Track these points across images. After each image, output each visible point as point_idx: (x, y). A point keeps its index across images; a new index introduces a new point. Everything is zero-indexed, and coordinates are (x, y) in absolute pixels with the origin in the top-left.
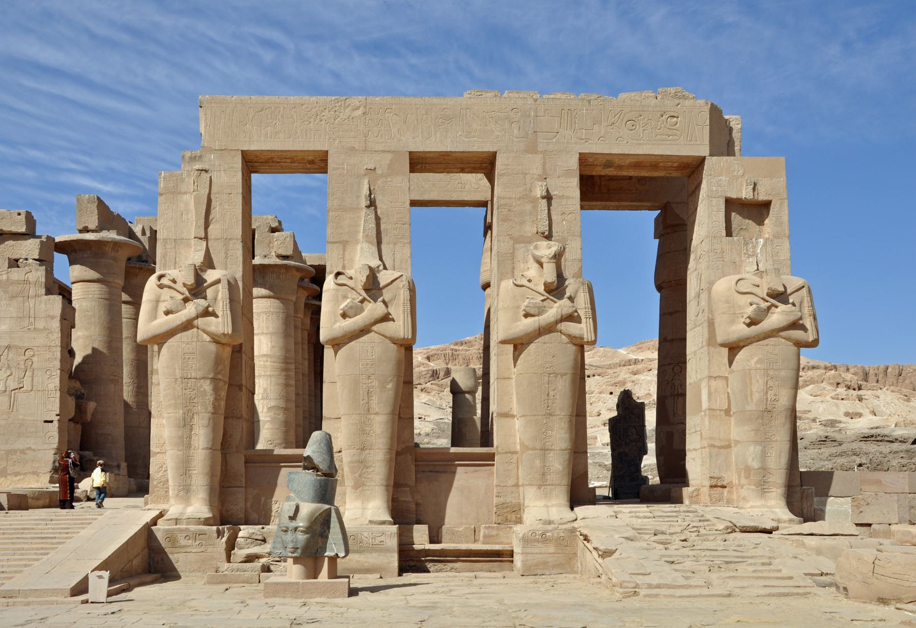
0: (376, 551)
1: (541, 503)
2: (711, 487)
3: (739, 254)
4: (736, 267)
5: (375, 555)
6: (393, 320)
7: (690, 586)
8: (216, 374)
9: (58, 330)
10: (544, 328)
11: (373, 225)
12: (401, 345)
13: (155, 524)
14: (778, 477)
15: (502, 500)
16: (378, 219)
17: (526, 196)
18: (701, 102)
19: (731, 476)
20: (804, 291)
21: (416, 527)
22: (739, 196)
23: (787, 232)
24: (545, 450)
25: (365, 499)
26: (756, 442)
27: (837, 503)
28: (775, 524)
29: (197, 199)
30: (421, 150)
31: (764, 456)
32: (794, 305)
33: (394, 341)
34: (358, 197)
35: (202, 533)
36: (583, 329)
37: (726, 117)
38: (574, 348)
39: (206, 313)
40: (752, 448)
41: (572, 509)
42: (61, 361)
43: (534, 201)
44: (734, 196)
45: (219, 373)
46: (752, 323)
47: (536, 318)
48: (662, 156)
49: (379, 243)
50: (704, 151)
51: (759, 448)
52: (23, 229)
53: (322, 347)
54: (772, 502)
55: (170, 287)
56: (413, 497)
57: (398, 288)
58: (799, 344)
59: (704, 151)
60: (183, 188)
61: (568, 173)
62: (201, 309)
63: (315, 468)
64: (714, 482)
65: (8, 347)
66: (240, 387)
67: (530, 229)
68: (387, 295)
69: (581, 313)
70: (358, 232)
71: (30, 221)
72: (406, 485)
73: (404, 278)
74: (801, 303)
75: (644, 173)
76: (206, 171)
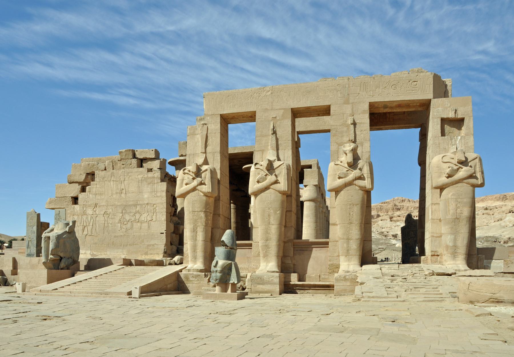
0: (270, 284)
1: (346, 263)
2: (432, 256)
3: (448, 145)
4: (446, 150)
5: (269, 285)
6: (279, 183)
7: (389, 297)
8: (206, 209)
9: (165, 196)
10: (347, 183)
11: (275, 142)
12: (284, 194)
13: (181, 272)
14: (462, 250)
15: (332, 262)
16: (277, 140)
17: (344, 124)
18: (429, 73)
19: (440, 251)
20: (477, 160)
21: (292, 274)
22: (448, 117)
23: (472, 132)
24: (348, 239)
25: (268, 261)
26: (451, 234)
27: (496, 263)
28: (454, 272)
29: (202, 137)
30: (296, 107)
31: (455, 240)
32: (471, 167)
33: (280, 192)
34: (269, 130)
35: (199, 276)
36: (366, 183)
37: (443, 80)
38: (362, 192)
39: (201, 184)
40: (449, 237)
41: (361, 266)
42: (167, 209)
43: (348, 126)
44: (445, 117)
45: (208, 209)
46: (449, 176)
47: (344, 179)
48: (410, 100)
49: (278, 150)
50: (430, 96)
51: (453, 236)
52: (154, 157)
53: (302, 203)
54: (459, 262)
55: (188, 174)
56: (292, 261)
57: (282, 169)
58: (474, 186)
59: (430, 96)
60: (197, 132)
61: (364, 112)
62: (199, 182)
63: (226, 246)
64: (433, 253)
65: (148, 204)
66: (219, 215)
67: (346, 139)
68: (277, 172)
69: (365, 175)
70: (268, 146)
71: (157, 153)
72: (289, 256)
73: (285, 164)
74: (475, 166)
75: (405, 110)
76: (206, 124)
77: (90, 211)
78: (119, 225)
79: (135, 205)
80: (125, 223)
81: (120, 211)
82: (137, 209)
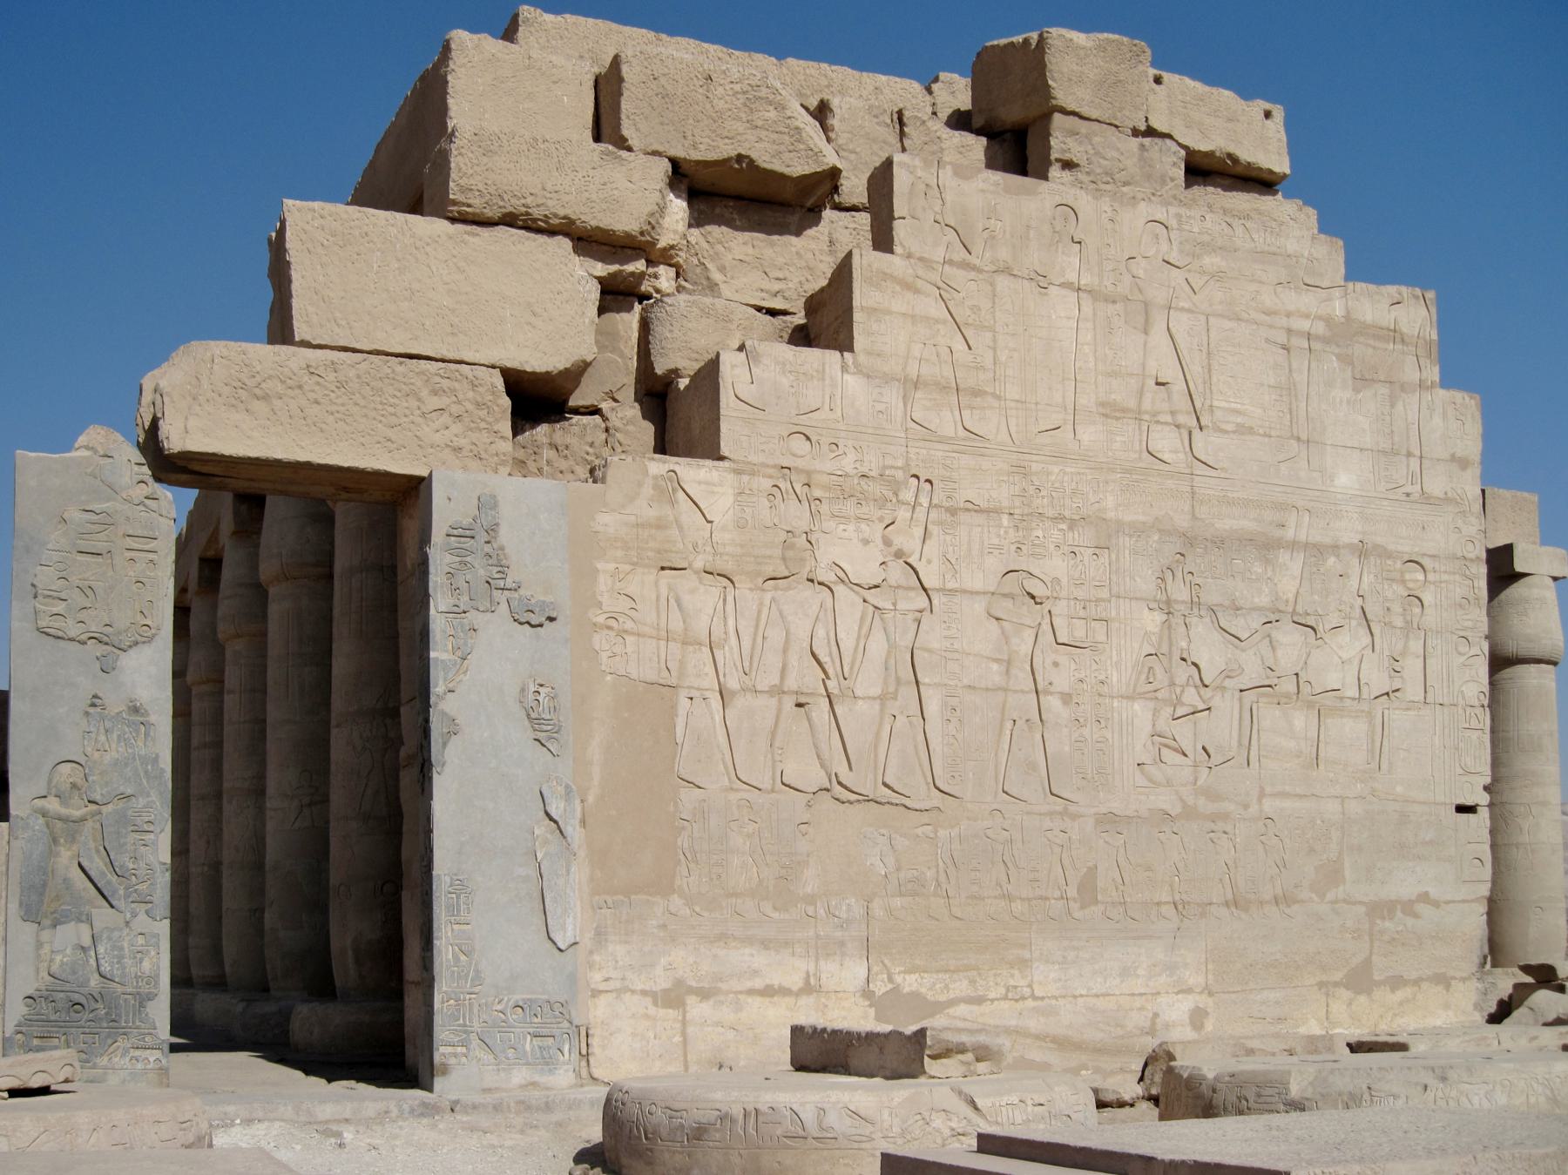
77: (848, 547)
78: (1140, 712)
79: (1266, 546)
80: (1191, 697)
81: (1145, 582)
82: (1288, 586)
